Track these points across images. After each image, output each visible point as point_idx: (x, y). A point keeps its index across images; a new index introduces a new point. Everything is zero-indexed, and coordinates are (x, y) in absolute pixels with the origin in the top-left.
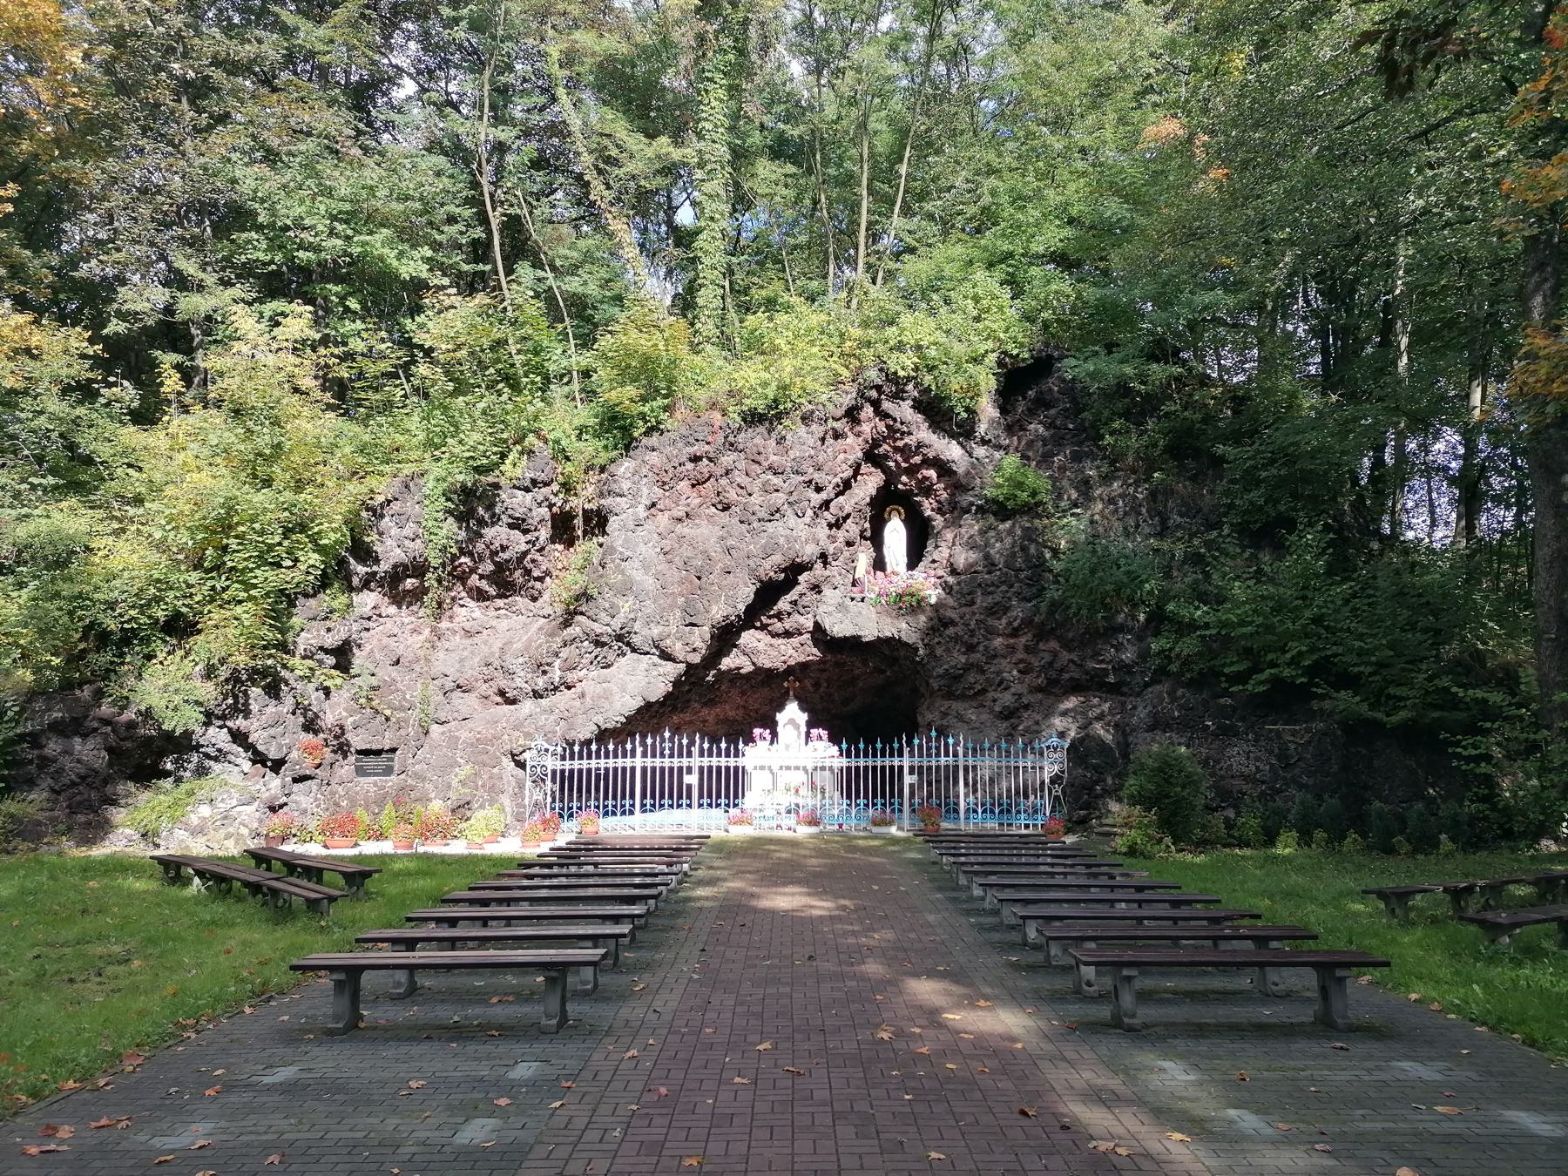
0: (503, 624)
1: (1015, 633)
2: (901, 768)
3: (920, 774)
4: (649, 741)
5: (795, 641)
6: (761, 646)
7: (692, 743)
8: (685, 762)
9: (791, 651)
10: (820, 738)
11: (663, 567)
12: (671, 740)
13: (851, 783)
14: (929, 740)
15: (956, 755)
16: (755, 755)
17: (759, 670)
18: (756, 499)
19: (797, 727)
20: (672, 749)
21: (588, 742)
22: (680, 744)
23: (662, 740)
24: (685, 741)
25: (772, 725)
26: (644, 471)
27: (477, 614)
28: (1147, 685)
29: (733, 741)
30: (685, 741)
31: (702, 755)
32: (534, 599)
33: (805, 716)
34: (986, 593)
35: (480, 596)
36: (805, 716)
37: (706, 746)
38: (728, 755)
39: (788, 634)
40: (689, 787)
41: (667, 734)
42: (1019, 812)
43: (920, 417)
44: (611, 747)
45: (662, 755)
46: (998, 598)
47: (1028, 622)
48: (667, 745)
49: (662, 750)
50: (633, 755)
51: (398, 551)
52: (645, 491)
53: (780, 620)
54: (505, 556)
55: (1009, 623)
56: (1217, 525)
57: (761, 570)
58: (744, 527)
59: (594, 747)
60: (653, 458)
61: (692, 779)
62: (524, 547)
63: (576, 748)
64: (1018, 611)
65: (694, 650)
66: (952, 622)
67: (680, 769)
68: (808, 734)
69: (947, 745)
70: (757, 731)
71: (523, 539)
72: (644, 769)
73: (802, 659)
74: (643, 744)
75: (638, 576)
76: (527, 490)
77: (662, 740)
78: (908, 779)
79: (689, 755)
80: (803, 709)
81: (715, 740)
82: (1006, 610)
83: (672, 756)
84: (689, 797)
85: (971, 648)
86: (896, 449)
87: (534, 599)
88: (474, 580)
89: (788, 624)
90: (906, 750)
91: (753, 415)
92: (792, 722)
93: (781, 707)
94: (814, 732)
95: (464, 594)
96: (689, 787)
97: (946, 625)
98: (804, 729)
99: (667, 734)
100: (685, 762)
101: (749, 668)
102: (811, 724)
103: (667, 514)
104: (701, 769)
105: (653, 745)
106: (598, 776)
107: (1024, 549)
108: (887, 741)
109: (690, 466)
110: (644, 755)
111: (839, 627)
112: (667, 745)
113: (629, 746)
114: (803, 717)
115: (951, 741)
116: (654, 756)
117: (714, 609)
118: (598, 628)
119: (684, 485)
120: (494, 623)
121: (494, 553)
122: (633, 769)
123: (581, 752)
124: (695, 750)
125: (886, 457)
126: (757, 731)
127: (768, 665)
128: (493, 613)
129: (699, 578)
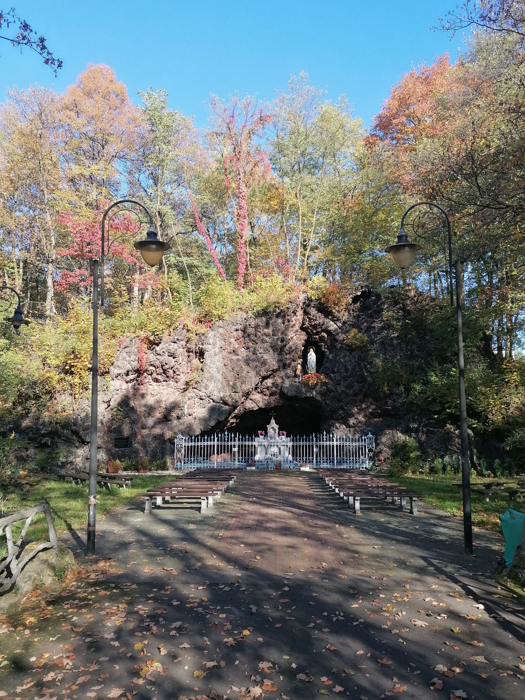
0: (165, 392)
1: (356, 395)
2: (313, 446)
3: (320, 448)
4: (220, 435)
7: (235, 436)
8: (233, 443)
10: (283, 435)
11: (225, 370)
12: (228, 435)
13: (295, 452)
14: (323, 435)
15: (333, 441)
16: (259, 441)
19: (275, 430)
20: (228, 438)
21: (198, 436)
22: (231, 437)
23: (225, 435)
24: (233, 435)
25: (266, 430)
26: (218, 335)
27: (156, 388)
28: (405, 415)
29: (250, 435)
30: (233, 435)
31: (239, 441)
32: (177, 382)
34: (345, 380)
35: (157, 380)
36: (278, 426)
38: (249, 441)
40: (235, 452)
41: (226, 433)
42: (356, 462)
43: (320, 314)
44: (206, 438)
45: (225, 441)
46: (349, 382)
47: (361, 391)
48: (226, 437)
49: (225, 438)
50: (214, 441)
51: (129, 365)
52: (218, 343)
54: (166, 367)
55: (354, 392)
56: (431, 355)
59: (200, 438)
60: (221, 330)
61: (236, 449)
62: (174, 363)
63: (193, 438)
64: (357, 387)
66: (333, 391)
67: (231, 446)
68: (279, 433)
69: (330, 437)
70: (259, 432)
71: (173, 360)
72: (218, 446)
74: (217, 436)
75: (215, 374)
76: (175, 342)
77: (225, 435)
78: (315, 450)
79: (235, 441)
80: (277, 423)
81: (244, 435)
82: (352, 386)
83: (228, 441)
84: (234, 456)
85: (340, 401)
87: (177, 382)
88: (155, 375)
90: (314, 439)
91: (258, 314)
92: (273, 428)
93: (269, 423)
95: (151, 381)
96: (235, 452)
97: (330, 392)
98: (277, 430)
99: (226, 433)
100: (233, 443)
104: (239, 446)
105: (221, 437)
106: (201, 448)
107: (359, 364)
108: (308, 436)
109: (235, 333)
110: (218, 441)
112: (226, 437)
113: (212, 437)
114: (276, 427)
115: (331, 436)
116: (221, 441)
118: (201, 394)
119: (232, 340)
120: (162, 391)
121: (162, 366)
122: (214, 446)
123: (195, 439)
124: (237, 439)
126: (259, 432)
128: (161, 387)
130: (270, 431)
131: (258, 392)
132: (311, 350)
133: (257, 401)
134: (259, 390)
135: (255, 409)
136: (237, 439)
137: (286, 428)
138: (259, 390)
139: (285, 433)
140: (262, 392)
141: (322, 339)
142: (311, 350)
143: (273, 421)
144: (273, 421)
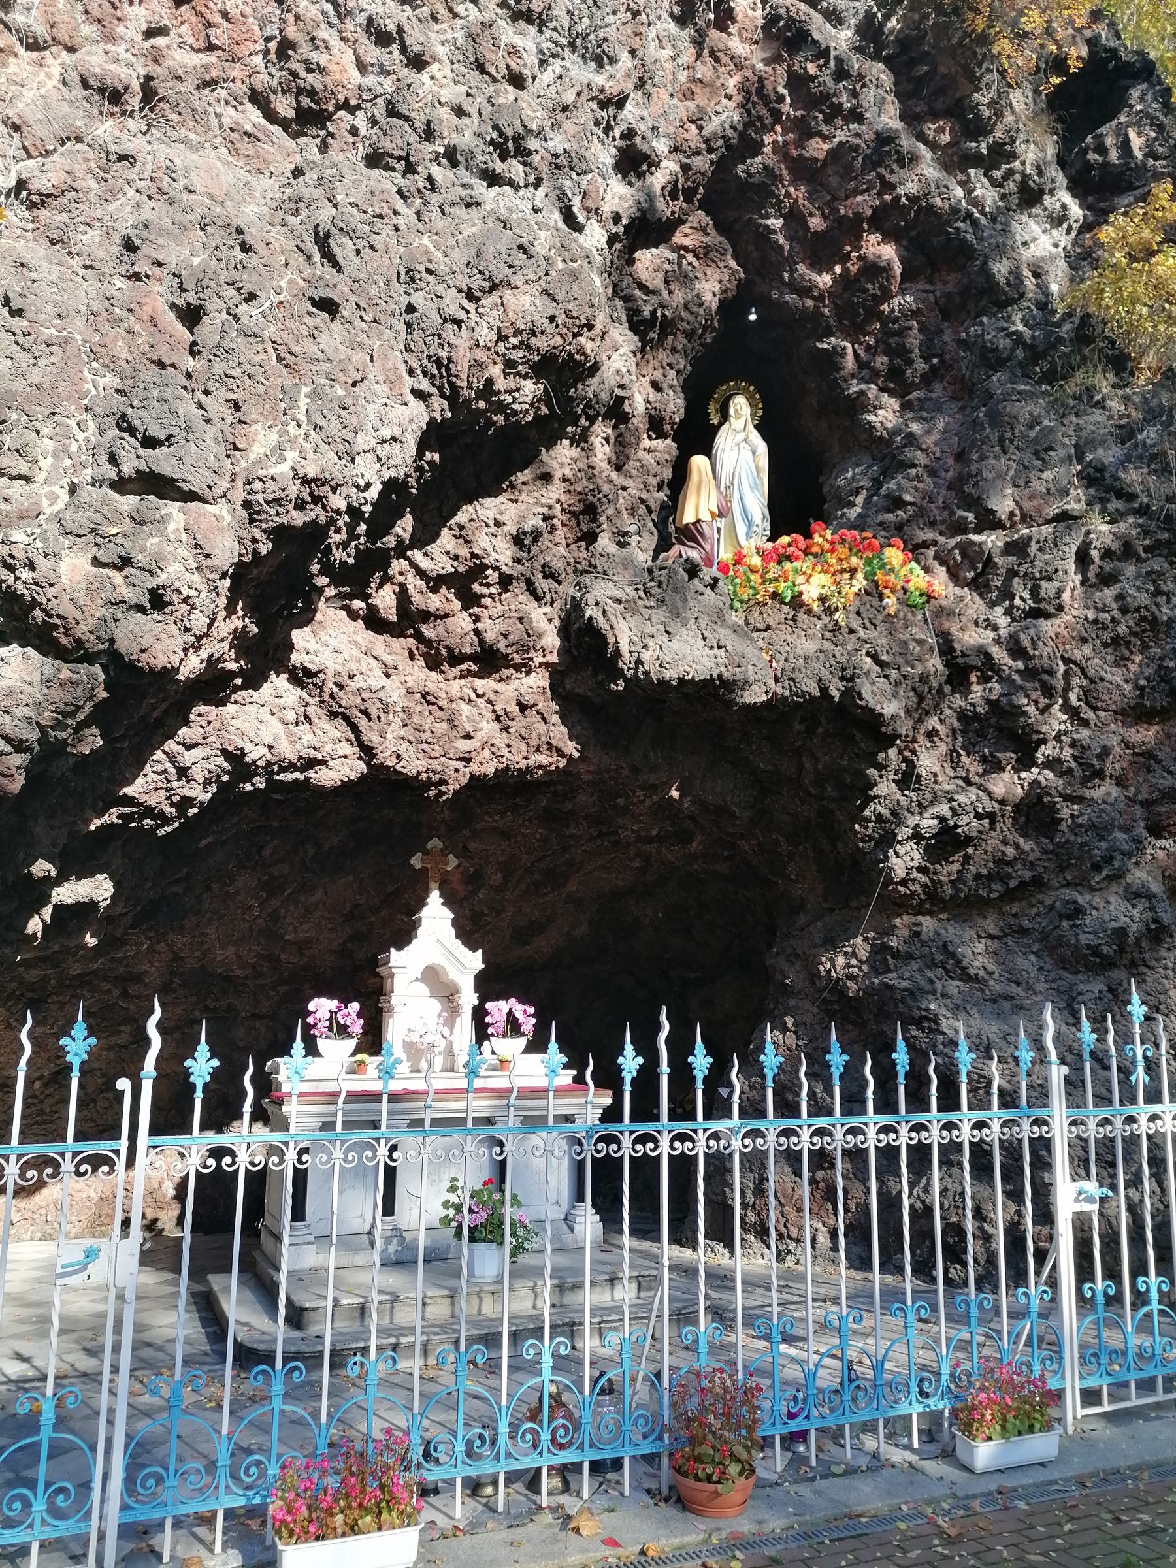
5: (510, 689)
6: (394, 693)
9: (488, 728)
10: (513, 1027)
17: (382, 786)
18: (440, 85)
24: (78, 1046)
30: (78, 1046)
33: (475, 961)
36: (475, 961)
37: (202, 1066)
39: (489, 660)
53: (470, 600)
57: (461, 340)
58: (387, 181)
65: (158, 600)
68: (479, 1014)
73: (519, 758)
86: (804, 170)
89: (495, 621)
94: (498, 1009)
98: (469, 998)
101: (343, 768)
102: (490, 985)
103: (56, 62)
111: (671, 649)
117: (261, 439)
124: (139, 1094)
125: (761, 193)
126: (322, 1007)
127: (414, 765)
129: (191, 316)
130: (411, 1010)
131: (374, 622)
132: (740, 406)
133: (352, 702)
134: (385, 600)
135: (324, 777)
136: (139, 1094)
137: (559, 979)
138: (385, 600)
139: (526, 1015)
140: (407, 621)
141: (857, 303)
142: (740, 406)
143: (436, 916)
144: (436, 916)
